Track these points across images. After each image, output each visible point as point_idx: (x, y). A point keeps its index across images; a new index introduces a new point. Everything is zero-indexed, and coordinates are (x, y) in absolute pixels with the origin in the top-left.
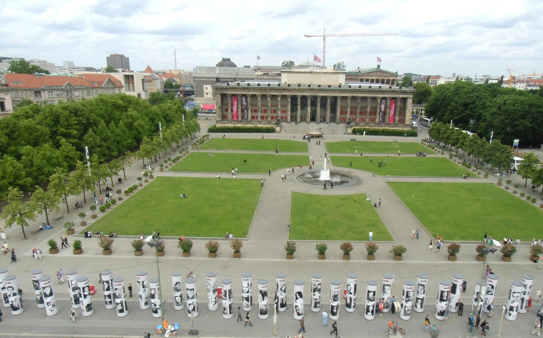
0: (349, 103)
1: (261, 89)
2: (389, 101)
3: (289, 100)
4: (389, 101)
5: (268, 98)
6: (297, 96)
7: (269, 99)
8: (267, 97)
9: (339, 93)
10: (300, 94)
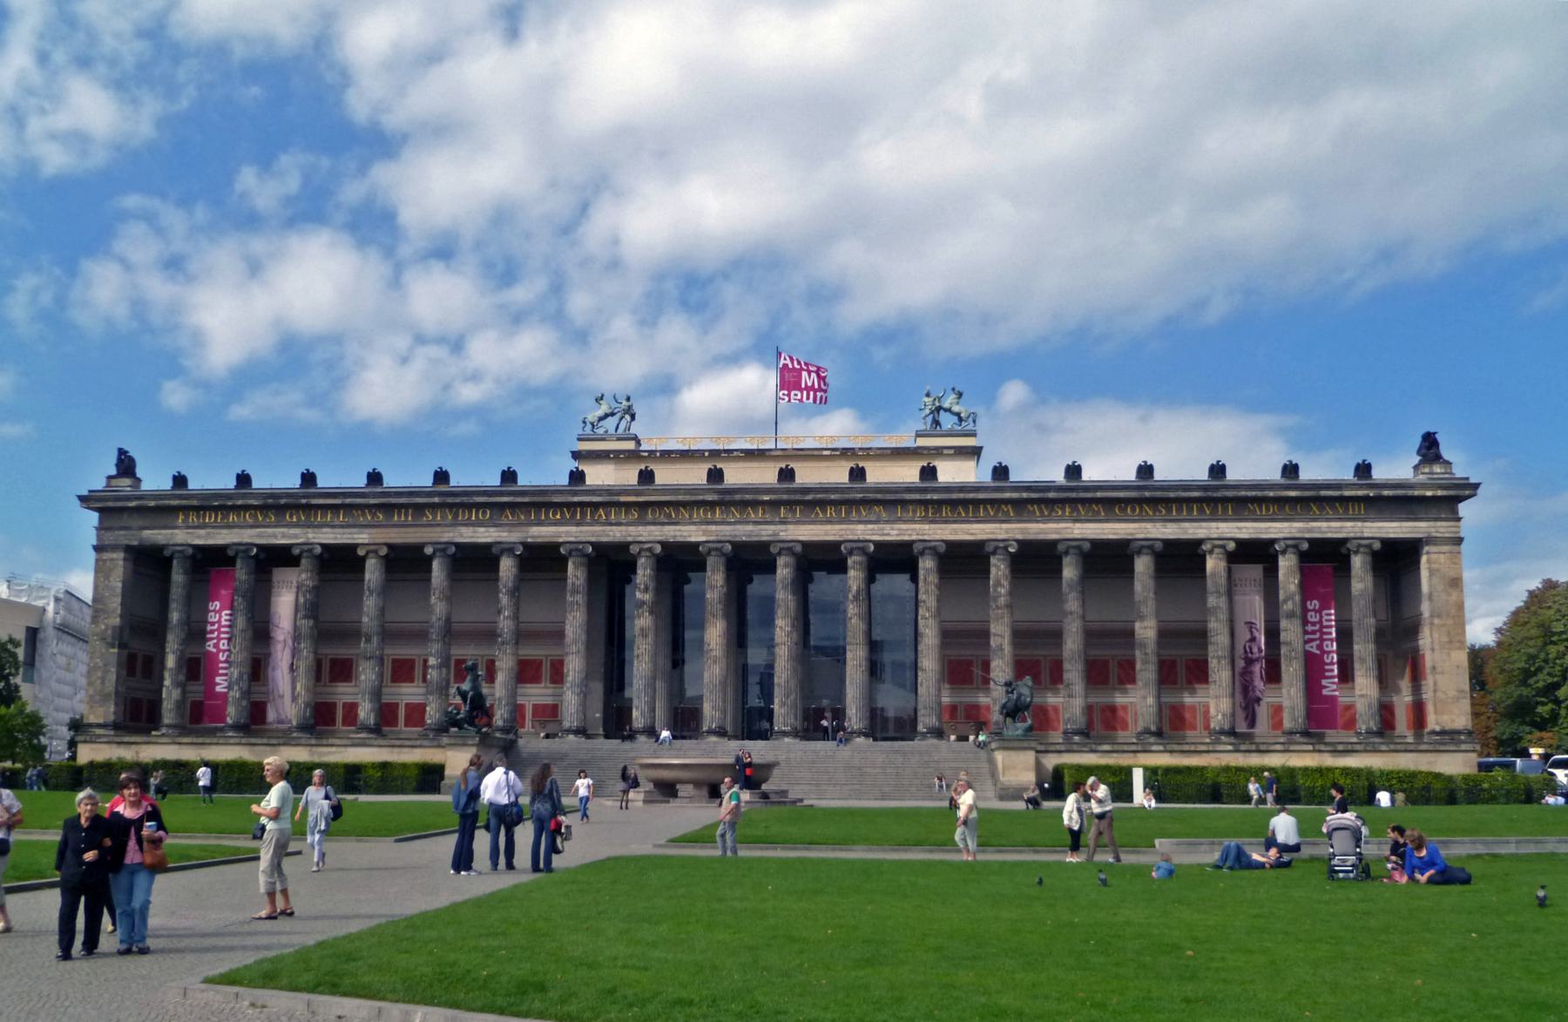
0: (1006, 583)
1: (388, 508)
2: (1287, 565)
3: (575, 573)
4: (1287, 565)
5: (436, 564)
6: (634, 549)
7: (438, 571)
8: (428, 560)
9: (925, 520)
10: (649, 534)
